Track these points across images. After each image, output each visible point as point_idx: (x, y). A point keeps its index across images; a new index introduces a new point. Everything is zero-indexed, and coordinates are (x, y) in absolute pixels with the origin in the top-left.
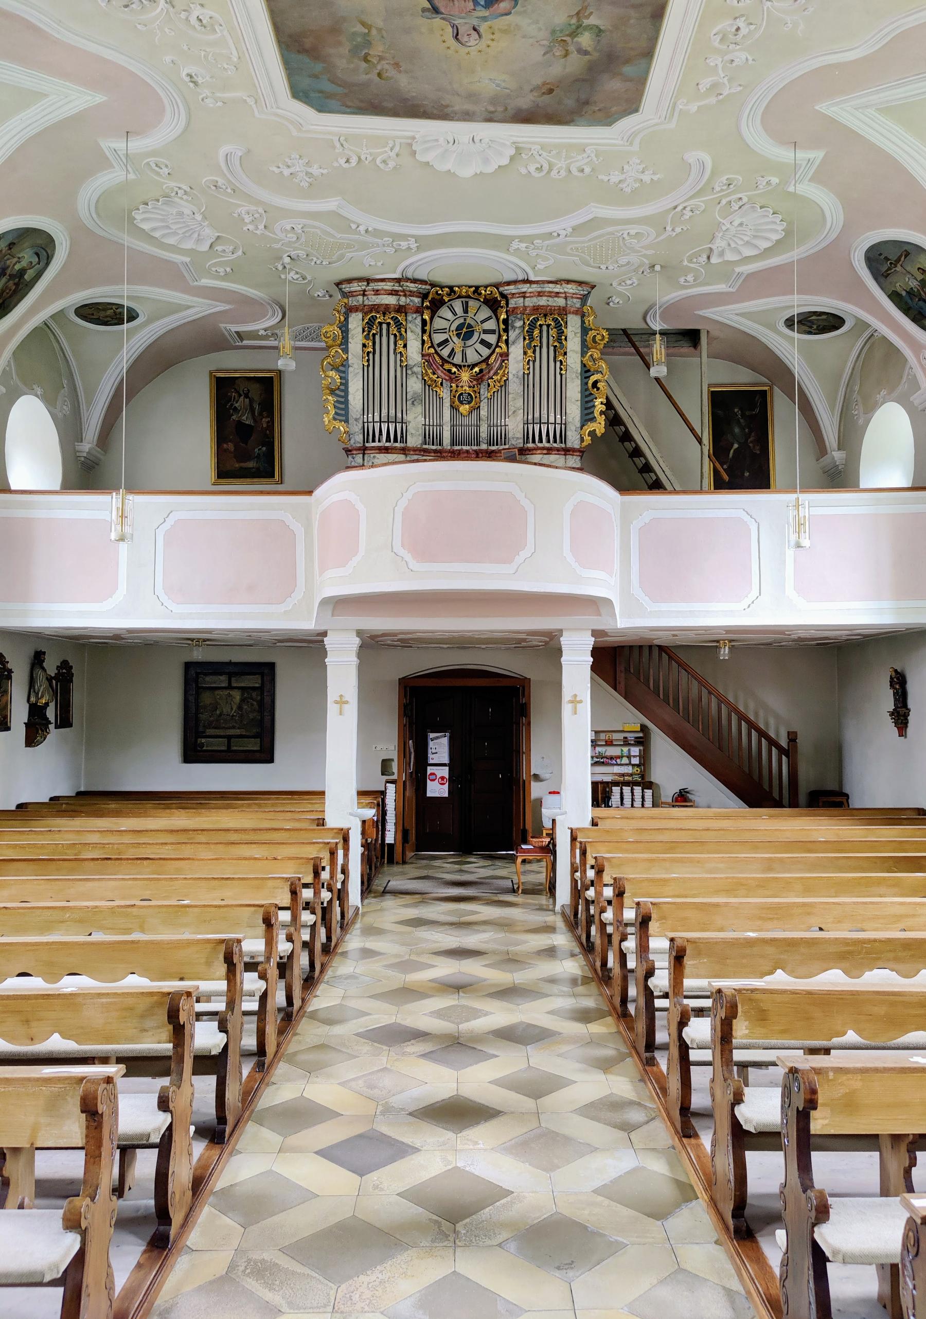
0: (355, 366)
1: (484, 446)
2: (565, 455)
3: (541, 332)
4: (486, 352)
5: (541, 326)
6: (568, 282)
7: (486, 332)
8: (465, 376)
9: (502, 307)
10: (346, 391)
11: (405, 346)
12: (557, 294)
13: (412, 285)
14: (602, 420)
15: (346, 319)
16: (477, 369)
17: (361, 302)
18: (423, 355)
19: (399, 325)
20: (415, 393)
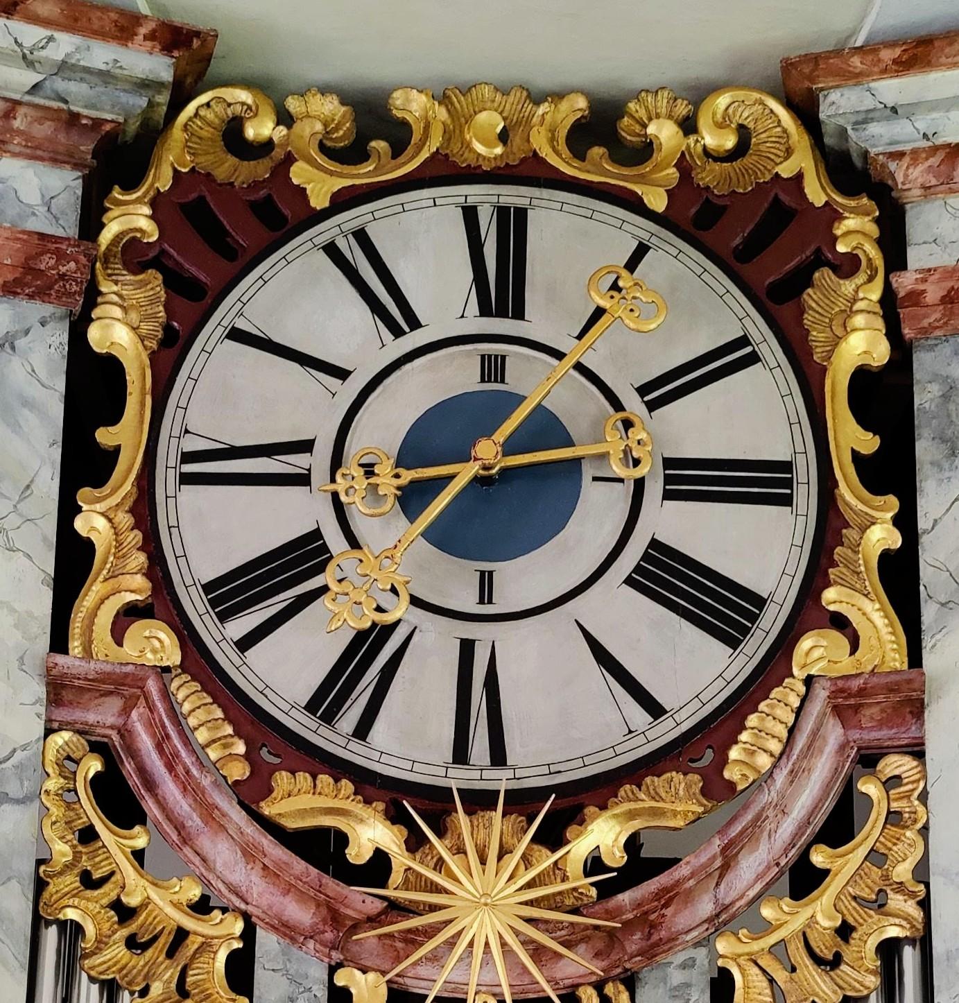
4: (690, 667)
7: (692, 479)
9: (848, 266)
18: (58, 690)
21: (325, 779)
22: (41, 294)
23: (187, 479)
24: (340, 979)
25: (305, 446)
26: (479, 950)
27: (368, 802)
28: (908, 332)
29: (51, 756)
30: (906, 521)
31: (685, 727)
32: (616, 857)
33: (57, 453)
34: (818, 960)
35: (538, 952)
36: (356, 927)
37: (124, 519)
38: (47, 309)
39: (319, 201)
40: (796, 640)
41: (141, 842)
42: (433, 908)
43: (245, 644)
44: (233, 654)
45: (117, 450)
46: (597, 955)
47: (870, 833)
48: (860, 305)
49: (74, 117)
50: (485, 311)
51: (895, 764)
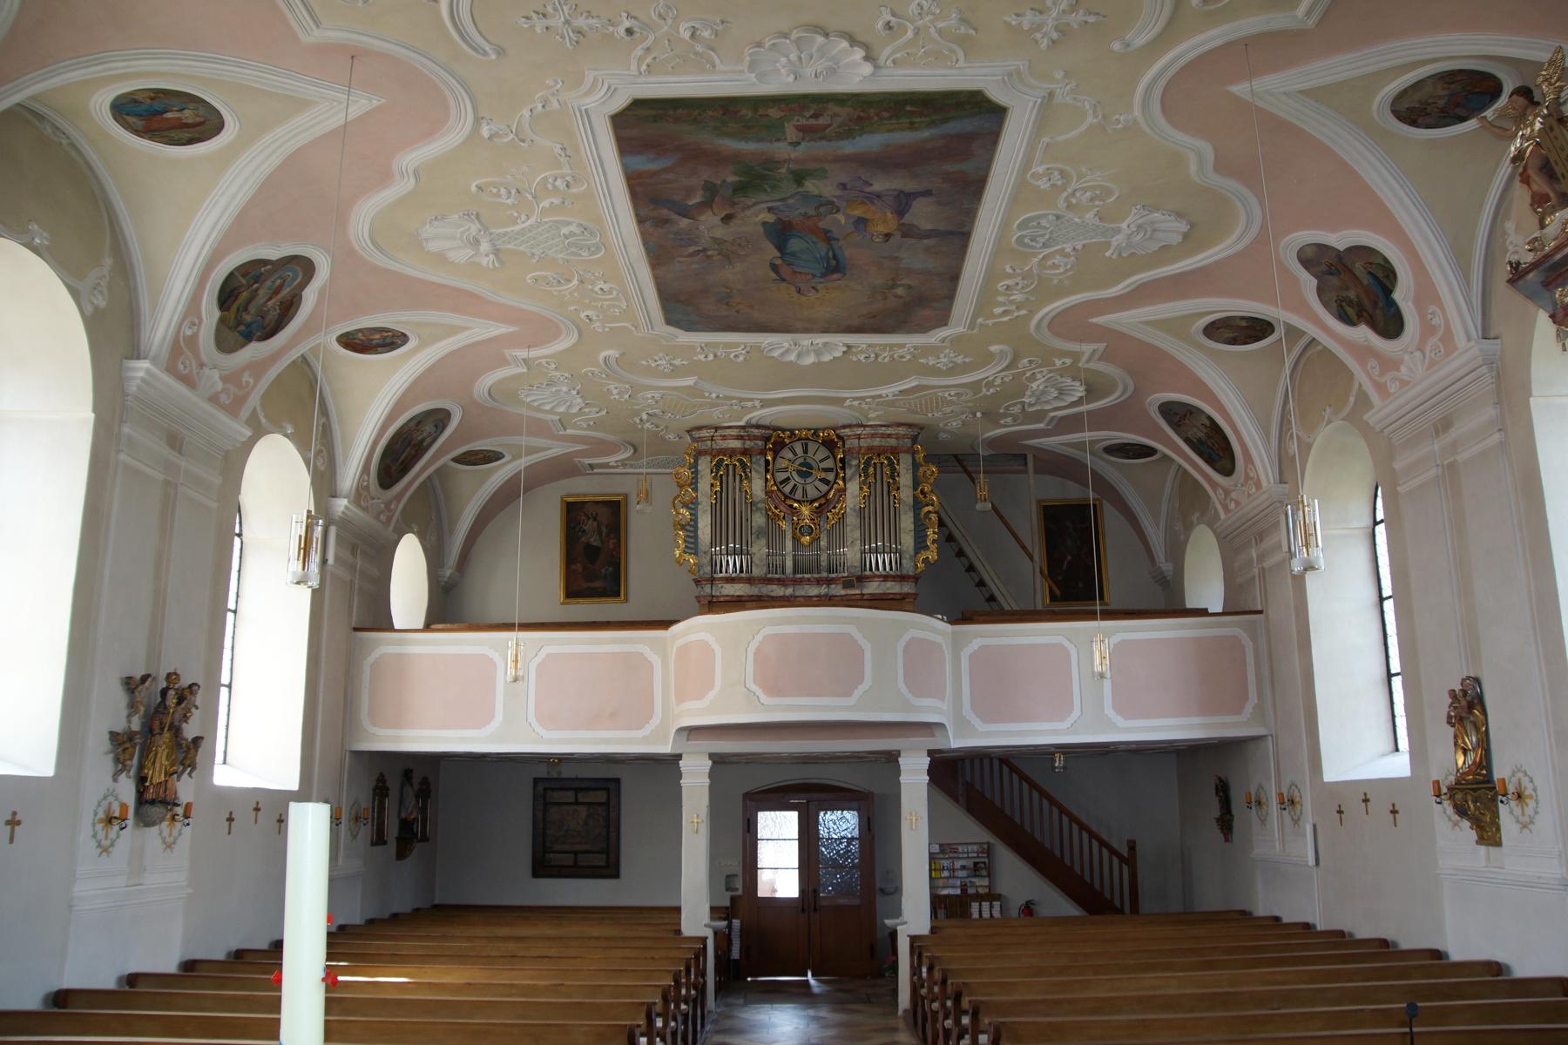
1: (825, 574)
4: (824, 488)
6: (899, 425)
8: (805, 511)
10: (696, 527)
12: (889, 436)
14: (933, 547)
15: (696, 461)
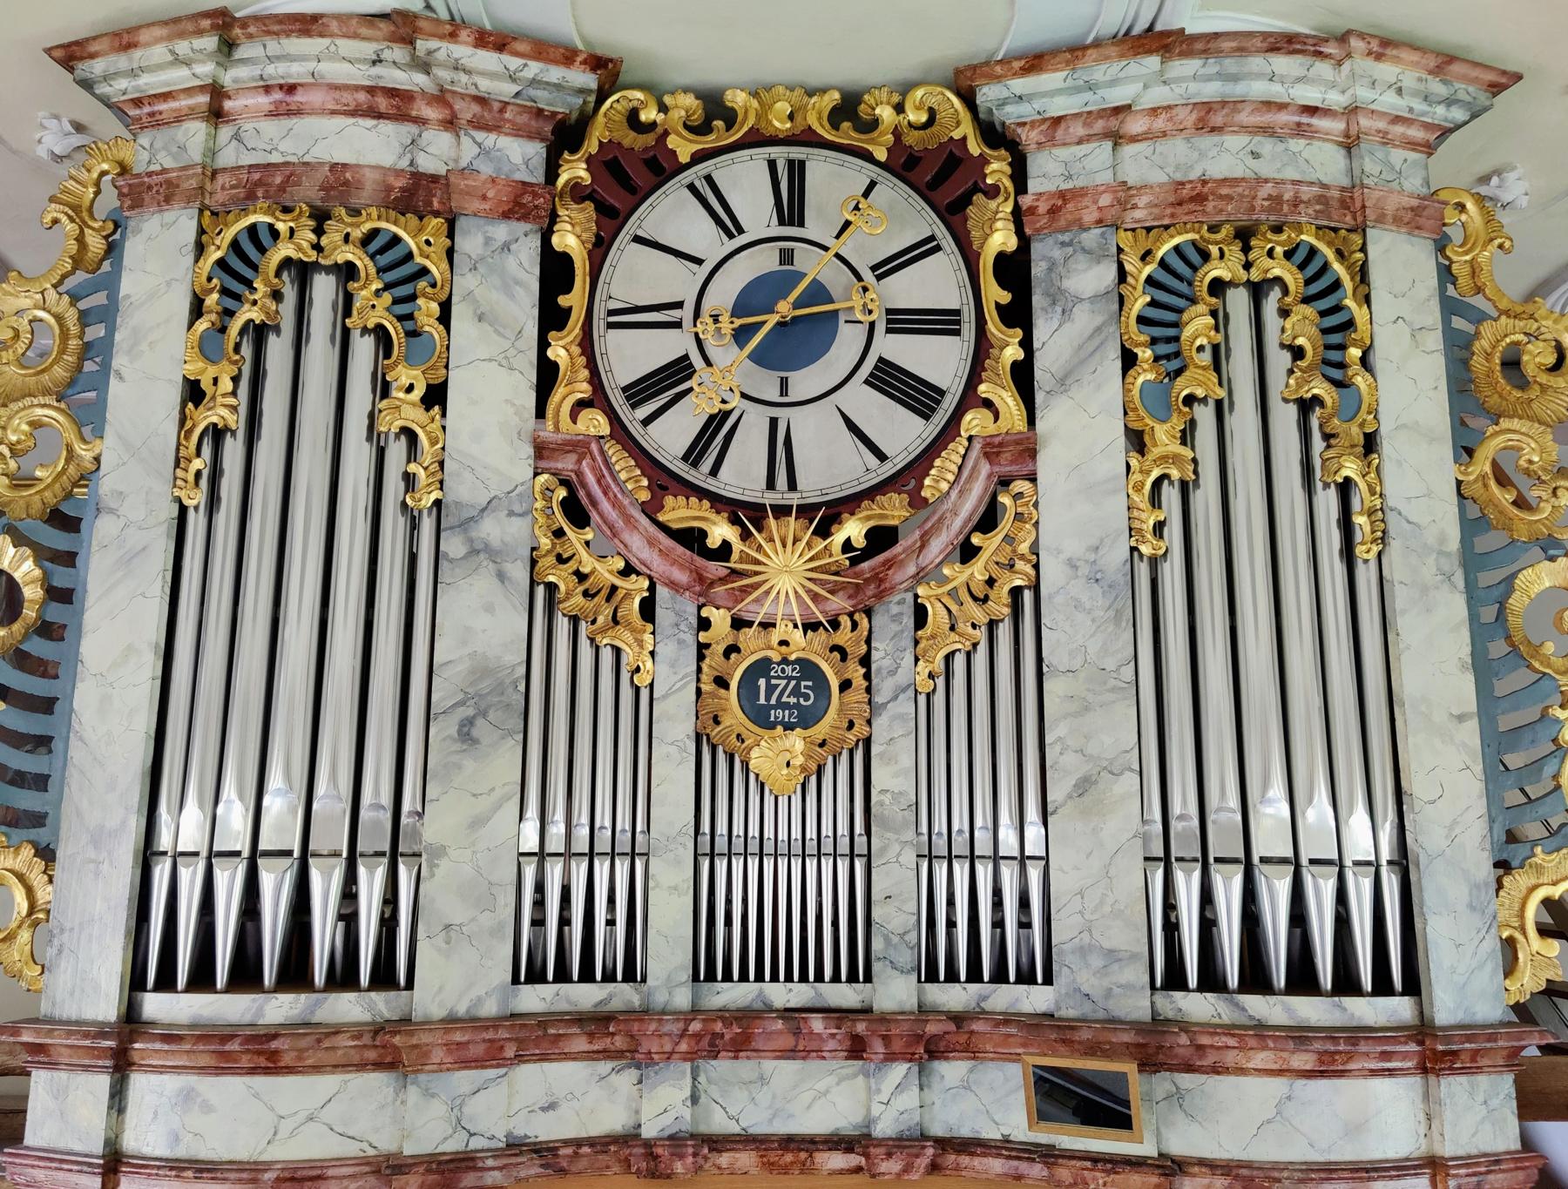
0: (133, 509)
2: (1424, 1070)
3: (1220, 319)
4: (902, 433)
5: (1218, 287)
7: (903, 321)
8: (786, 570)
9: (993, 192)
11: (436, 396)
13: (487, 59)
16: (853, 529)
17: (196, 154)
18: (541, 450)
19: (404, 278)
20: (482, 670)
21: (693, 500)
22: (524, 218)
23: (611, 326)
24: (704, 613)
25: (679, 305)
26: (782, 597)
27: (718, 512)
28: (1028, 231)
29: (537, 489)
30: (1027, 344)
31: (899, 467)
32: (859, 542)
33: (536, 312)
34: (975, 599)
35: (815, 597)
36: (712, 584)
37: (576, 350)
38: (527, 226)
39: (684, 158)
40: (962, 415)
41: (590, 536)
42: (757, 573)
43: (647, 422)
44: (639, 427)
45: (570, 309)
46: (850, 597)
47: (1006, 525)
48: (1000, 215)
49: (540, 111)
50: (781, 222)
51: (1021, 486)
